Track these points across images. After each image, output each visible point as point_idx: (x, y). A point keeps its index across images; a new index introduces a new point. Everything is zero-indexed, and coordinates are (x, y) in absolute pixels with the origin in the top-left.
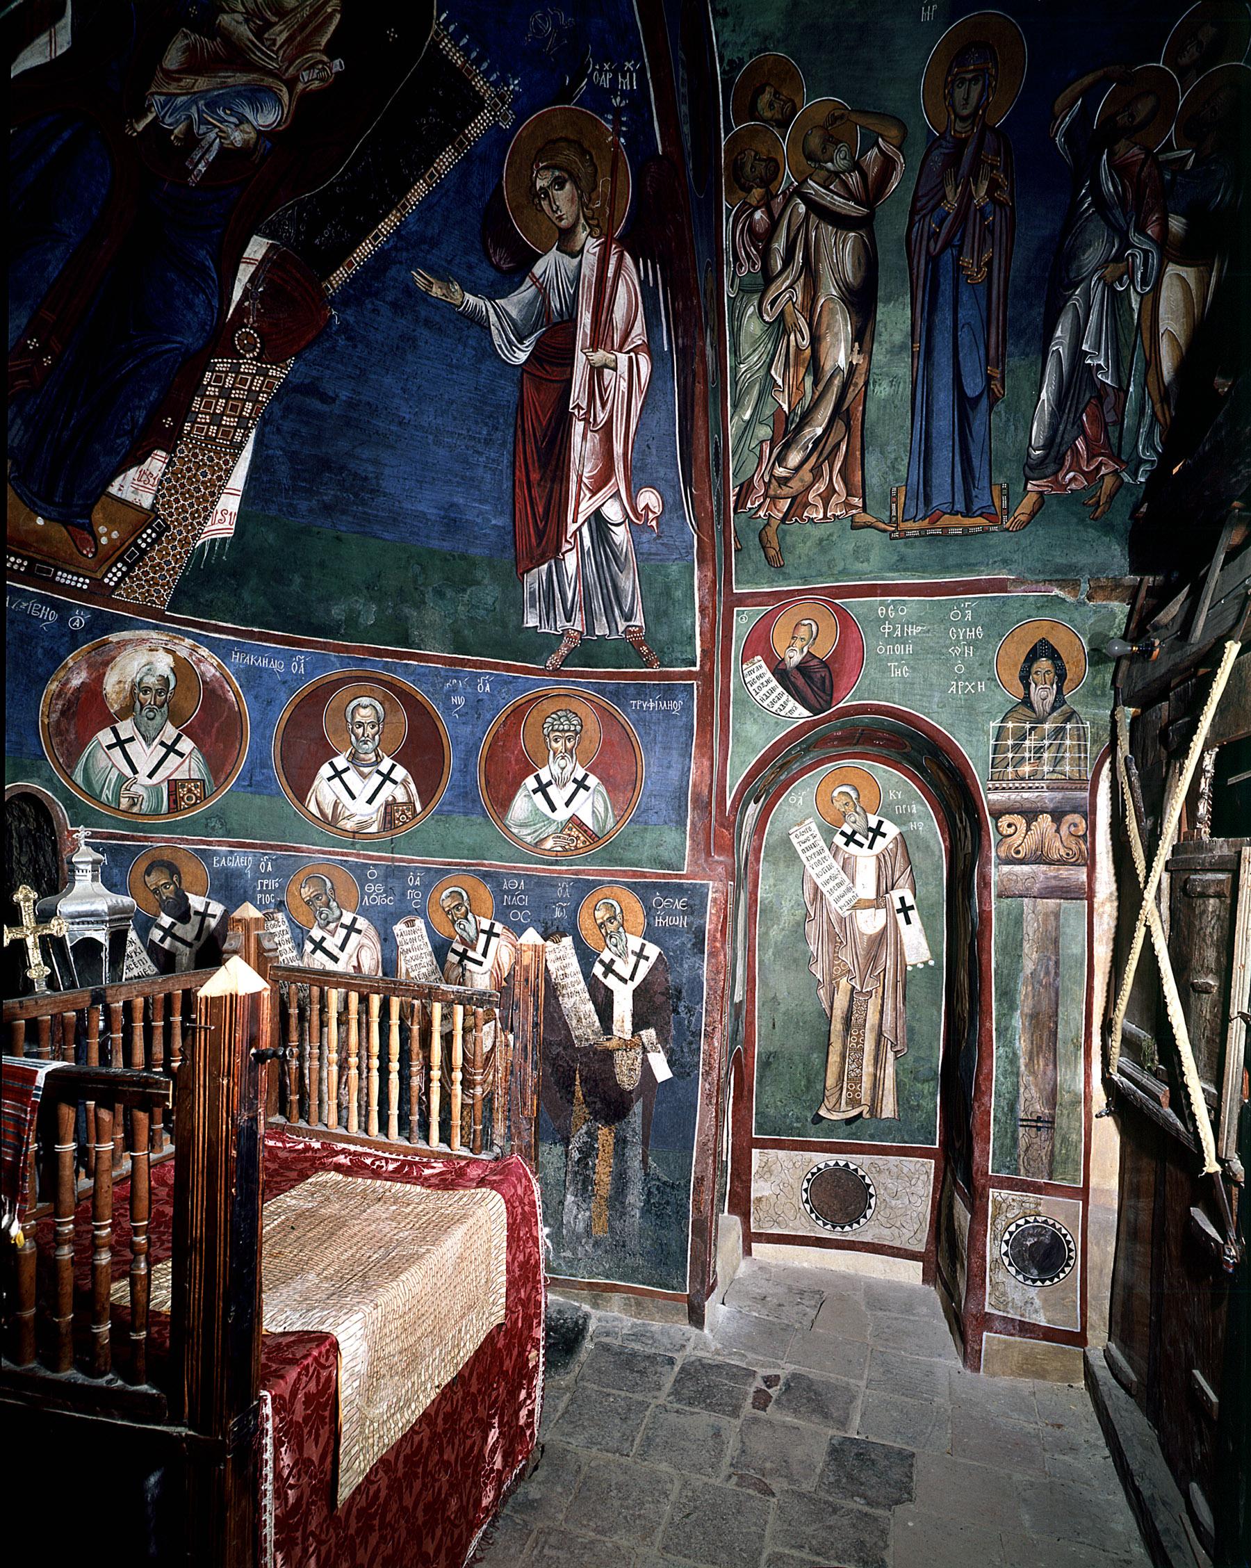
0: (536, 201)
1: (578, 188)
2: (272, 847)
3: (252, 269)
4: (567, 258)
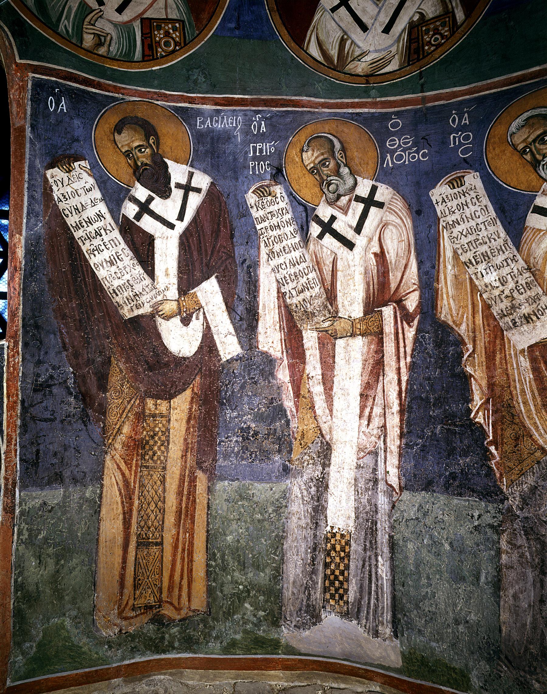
2: (266, 103)
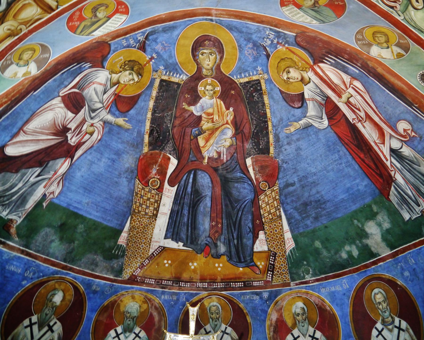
0: (289, 82)
1: (292, 67)
3: (251, 167)
4: (309, 85)
